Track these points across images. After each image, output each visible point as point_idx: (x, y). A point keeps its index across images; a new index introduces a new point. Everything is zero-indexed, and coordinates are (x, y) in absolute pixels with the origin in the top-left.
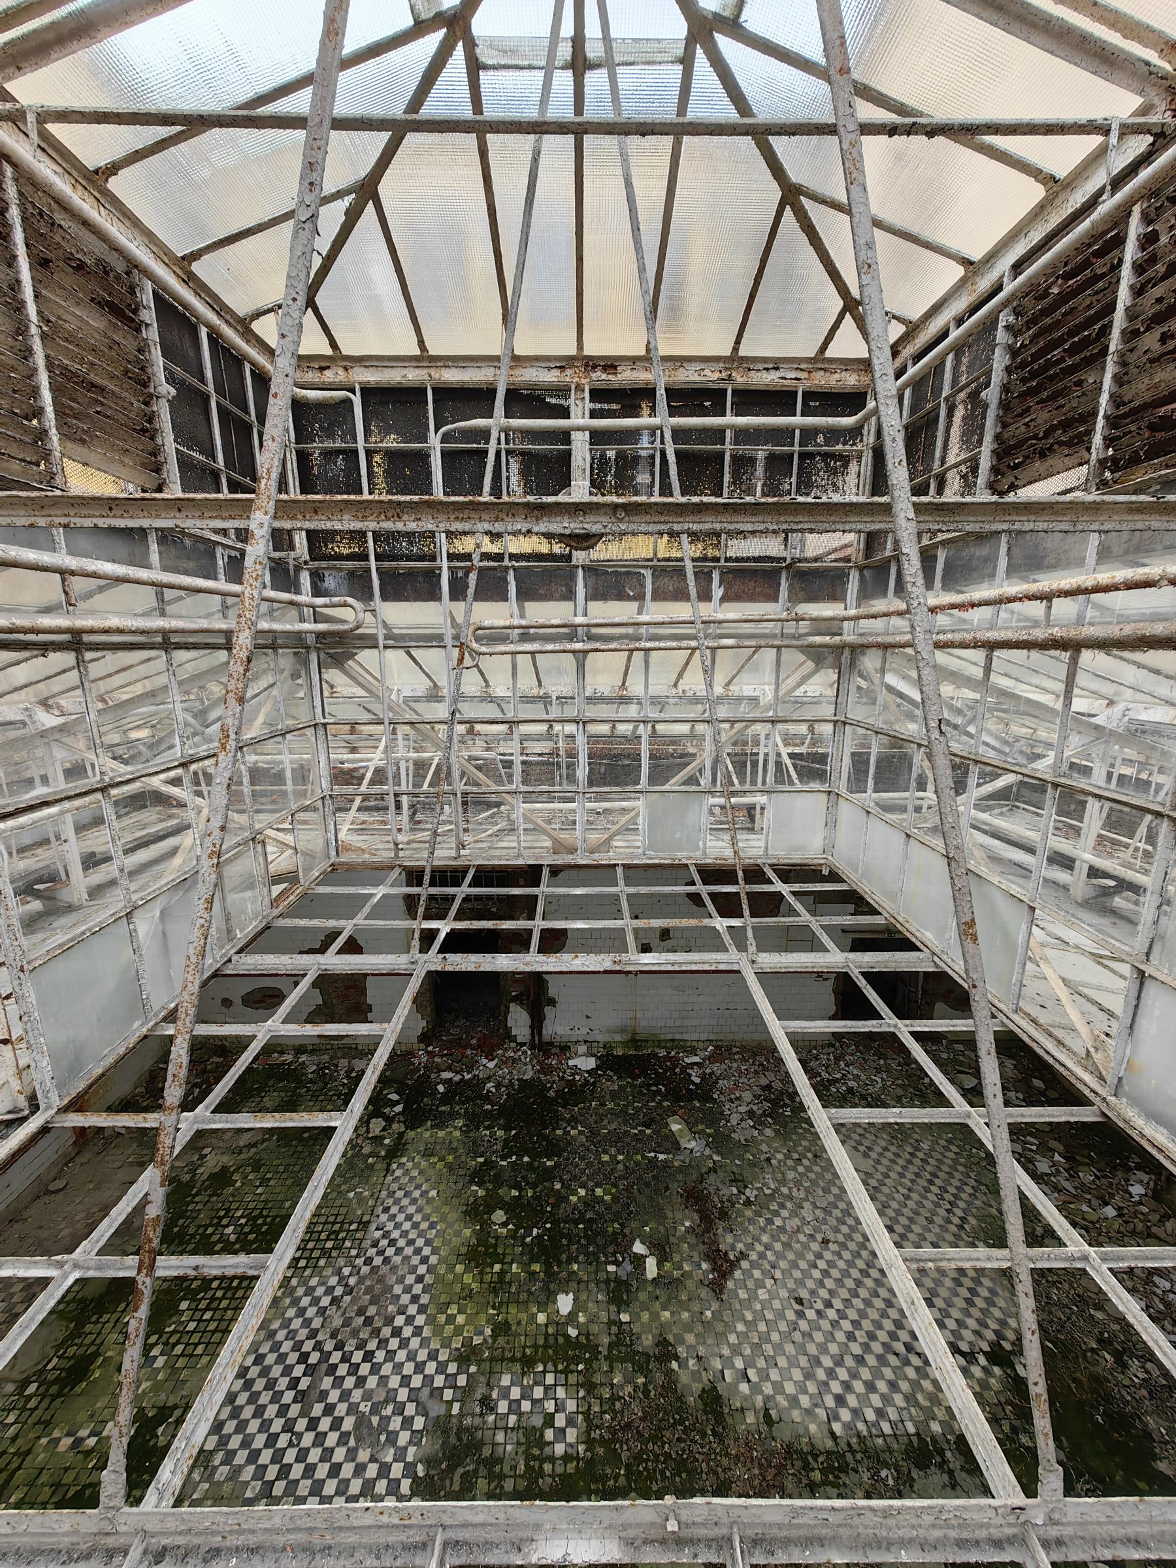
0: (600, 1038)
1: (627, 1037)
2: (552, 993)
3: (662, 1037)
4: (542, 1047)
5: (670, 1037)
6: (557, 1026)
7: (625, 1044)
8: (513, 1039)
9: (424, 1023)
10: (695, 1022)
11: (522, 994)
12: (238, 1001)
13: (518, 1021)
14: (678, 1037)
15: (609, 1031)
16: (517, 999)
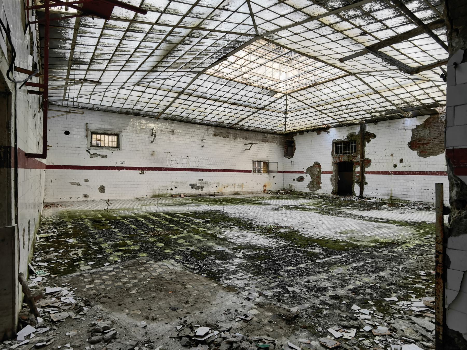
0: (381, 197)
1: (388, 197)
2: (367, 180)
3: (401, 198)
4: (361, 197)
5: (403, 199)
6: (366, 193)
7: (388, 200)
8: (355, 195)
9: (333, 188)
10: (413, 194)
11: (358, 180)
12: (296, 180)
13: (356, 188)
14: (406, 199)
15: (383, 195)
16: (357, 182)
